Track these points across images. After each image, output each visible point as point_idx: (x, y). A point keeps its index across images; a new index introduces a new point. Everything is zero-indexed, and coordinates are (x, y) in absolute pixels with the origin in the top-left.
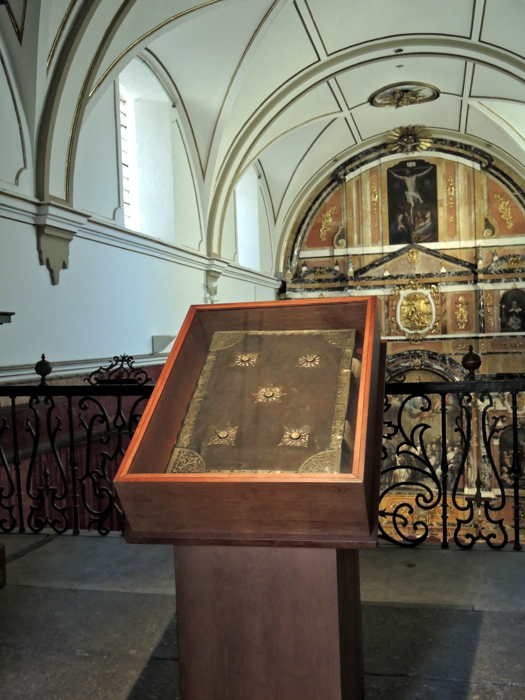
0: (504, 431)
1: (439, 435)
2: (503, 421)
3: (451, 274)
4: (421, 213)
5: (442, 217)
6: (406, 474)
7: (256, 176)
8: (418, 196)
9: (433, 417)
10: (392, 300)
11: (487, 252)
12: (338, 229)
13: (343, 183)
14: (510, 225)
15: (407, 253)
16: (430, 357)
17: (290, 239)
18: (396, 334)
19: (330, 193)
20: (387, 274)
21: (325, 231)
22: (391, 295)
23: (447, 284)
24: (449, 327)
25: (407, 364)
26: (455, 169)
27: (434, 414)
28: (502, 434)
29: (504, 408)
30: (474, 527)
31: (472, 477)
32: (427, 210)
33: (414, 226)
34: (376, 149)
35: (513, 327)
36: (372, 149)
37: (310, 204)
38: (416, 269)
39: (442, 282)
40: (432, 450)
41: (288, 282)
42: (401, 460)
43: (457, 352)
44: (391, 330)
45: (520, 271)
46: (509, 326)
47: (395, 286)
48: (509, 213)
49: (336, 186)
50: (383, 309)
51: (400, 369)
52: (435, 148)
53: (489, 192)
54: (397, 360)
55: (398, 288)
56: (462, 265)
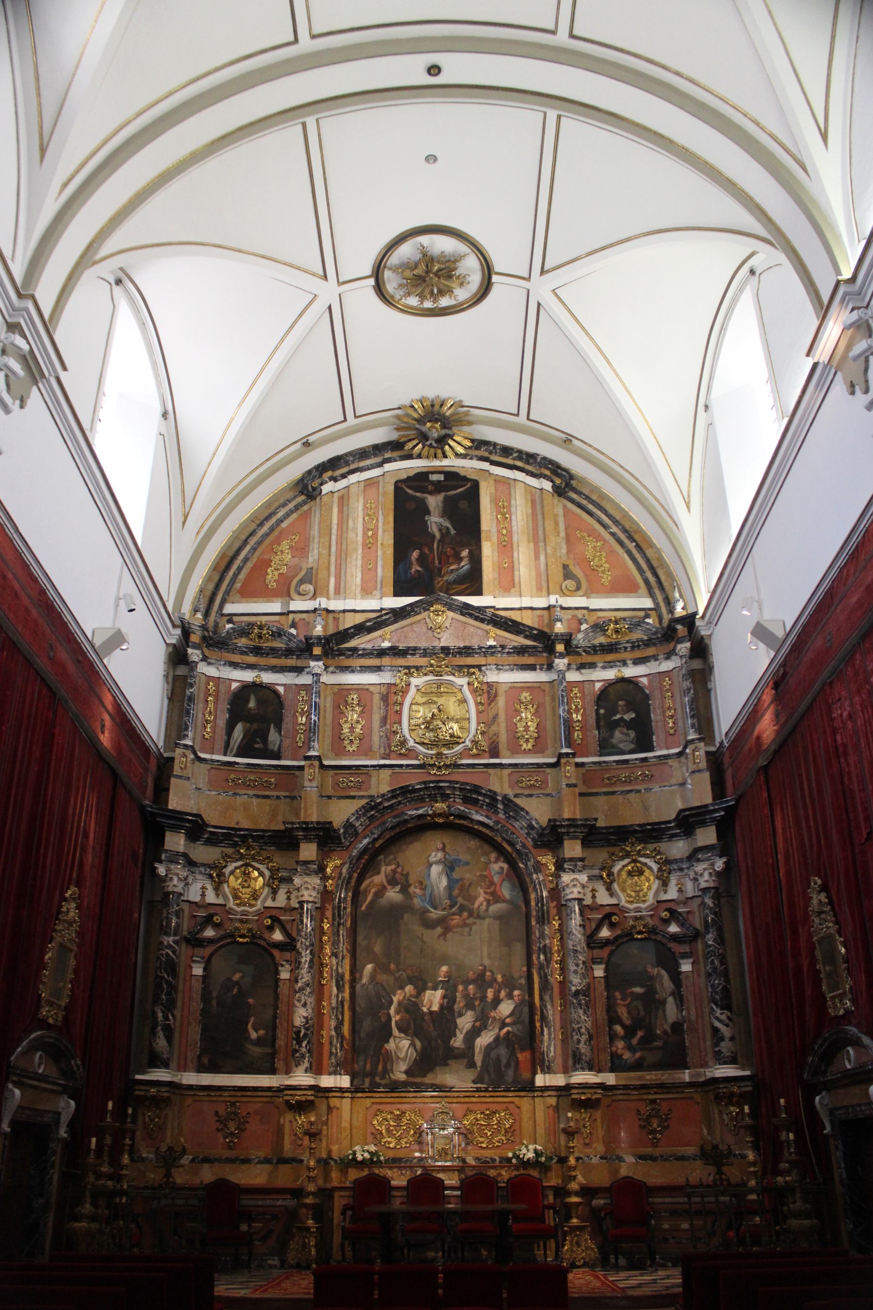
0: (614, 948)
1: (481, 965)
2: (612, 926)
4: (452, 548)
5: (488, 557)
7: (159, 411)
8: (447, 524)
9: (470, 926)
10: (395, 693)
11: (570, 617)
12: (301, 569)
14: (606, 579)
15: (426, 613)
16: (466, 800)
17: (208, 579)
18: (402, 756)
19: (291, 512)
20: (386, 644)
21: (276, 573)
23: (500, 669)
25: (421, 812)
26: (509, 488)
28: (612, 953)
29: (613, 901)
30: (558, 1162)
31: (552, 1049)
32: (464, 546)
33: (440, 570)
34: (377, 449)
35: (622, 746)
37: (253, 526)
38: (442, 640)
40: (466, 996)
41: (193, 633)
42: (401, 1020)
44: (390, 746)
46: (613, 746)
48: (604, 560)
49: (304, 503)
50: (375, 709)
51: (406, 821)
52: (477, 456)
53: (567, 528)
54: (400, 803)
56: (526, 637)
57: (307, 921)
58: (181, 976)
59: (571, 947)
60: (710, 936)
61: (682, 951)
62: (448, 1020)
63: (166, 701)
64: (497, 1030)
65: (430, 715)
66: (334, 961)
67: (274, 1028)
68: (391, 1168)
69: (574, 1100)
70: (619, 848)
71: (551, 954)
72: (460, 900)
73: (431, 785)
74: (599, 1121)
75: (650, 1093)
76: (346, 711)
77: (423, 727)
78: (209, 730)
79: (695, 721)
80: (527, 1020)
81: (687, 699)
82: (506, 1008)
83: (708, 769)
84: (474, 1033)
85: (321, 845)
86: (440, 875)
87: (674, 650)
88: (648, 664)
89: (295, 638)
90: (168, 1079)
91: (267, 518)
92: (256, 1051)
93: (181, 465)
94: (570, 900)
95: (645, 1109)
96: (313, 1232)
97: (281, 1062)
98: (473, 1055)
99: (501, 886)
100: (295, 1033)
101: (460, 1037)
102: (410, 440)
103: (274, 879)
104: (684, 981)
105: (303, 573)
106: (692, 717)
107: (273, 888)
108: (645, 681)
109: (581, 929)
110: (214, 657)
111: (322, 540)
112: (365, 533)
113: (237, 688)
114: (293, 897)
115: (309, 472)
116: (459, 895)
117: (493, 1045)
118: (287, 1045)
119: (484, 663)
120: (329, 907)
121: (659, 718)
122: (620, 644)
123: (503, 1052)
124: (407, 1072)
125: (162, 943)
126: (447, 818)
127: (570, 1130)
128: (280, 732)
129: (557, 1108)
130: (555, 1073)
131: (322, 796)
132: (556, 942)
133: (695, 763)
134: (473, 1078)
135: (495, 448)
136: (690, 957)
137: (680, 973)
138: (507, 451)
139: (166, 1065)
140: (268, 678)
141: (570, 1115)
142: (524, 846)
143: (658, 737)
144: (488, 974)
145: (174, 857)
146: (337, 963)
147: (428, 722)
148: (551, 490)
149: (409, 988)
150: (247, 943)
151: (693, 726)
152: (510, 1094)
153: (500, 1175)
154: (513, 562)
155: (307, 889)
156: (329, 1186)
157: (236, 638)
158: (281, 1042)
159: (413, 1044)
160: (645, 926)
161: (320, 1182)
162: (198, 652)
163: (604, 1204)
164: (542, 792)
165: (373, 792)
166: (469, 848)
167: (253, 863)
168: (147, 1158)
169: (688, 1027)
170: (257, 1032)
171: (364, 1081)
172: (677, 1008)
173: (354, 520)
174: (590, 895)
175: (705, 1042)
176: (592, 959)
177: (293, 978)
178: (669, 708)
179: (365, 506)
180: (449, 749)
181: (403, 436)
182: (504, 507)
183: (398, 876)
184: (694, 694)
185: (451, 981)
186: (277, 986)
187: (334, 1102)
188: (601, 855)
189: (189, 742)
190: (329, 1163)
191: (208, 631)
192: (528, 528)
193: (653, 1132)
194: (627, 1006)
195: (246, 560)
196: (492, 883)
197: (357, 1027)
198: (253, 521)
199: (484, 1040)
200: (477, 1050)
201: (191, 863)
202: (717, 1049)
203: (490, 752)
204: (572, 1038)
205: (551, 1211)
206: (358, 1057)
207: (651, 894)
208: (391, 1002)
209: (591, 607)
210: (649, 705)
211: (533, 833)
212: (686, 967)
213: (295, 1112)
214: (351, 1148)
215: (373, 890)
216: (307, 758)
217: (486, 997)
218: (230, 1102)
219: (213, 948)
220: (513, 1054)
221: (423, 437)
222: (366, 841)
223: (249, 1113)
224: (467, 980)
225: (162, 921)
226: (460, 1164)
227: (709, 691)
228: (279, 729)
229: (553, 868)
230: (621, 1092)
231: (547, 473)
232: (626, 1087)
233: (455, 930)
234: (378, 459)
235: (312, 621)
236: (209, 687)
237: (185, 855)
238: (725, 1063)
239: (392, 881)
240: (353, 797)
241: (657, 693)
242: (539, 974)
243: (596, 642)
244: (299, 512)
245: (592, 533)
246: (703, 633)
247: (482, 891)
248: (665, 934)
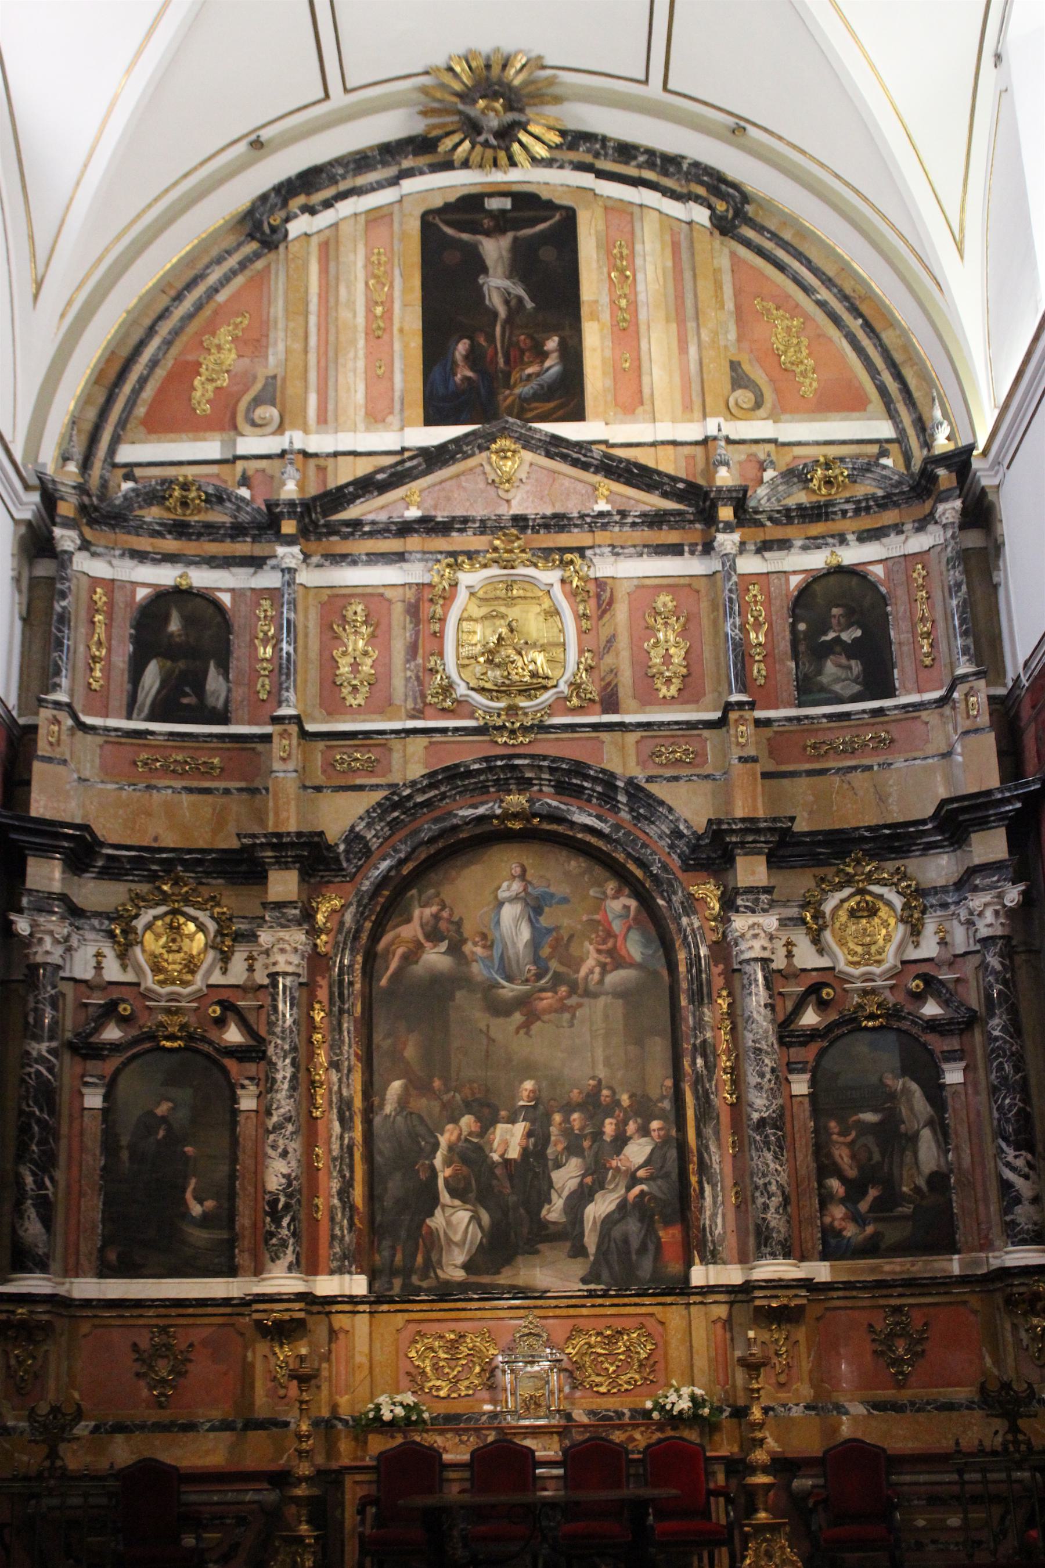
1: (593, 1078)
2: (823, 1005)
3: (630, 520)
4: (531, 337)
5: (594, 350)
8: (520, 291)
9: (572, 1010)
10: (431, 600)
11: (743, 457)
12: (255, 378)
13: (277, 247)
14: (809, 386)
15: (485, 454)
16: (562, 789)
17: (85, 400)
18: (445, 712)
19: (234, 273)
20: (413, 513)
22: (430, 585)
23: (617, 554)
24: (625, 693)
25: (481, 810)
26: (632, 222)
27: (573, 1000)
28: (822, 1053)
29: (824, 962)
30: (731, 1416)
31: (719, 1221)
33: (507, 375)
34: (389, 151)
35: (837, 688)
36: (376, 153)
37: (164, 301)
38: (514, 503)
39: (600, 546)
40: (567, 1132)
41: (62, 499)
44: (423, 696)
45: (850, 506)
46: (822, 689)
47: (439, 557)
48: (805, 352)
49: (257, 256)
50: (396, 630)
51: (455, 828)
52: (571, 162)
53: (737, 293)
55: (451, 560)
56: (665, 495)
57: (284, 1007)
58: (65, 1112)
59: (750, 1043)
60: (996, 1021)
61: (945, 1048)
62: (536, 1174)
63: (18, 625)
64: (623, 1191)
65: (495, 639)
66: (334, 1076)
67: (232, 1196)
68: (442, 1432)
69: (758, 1309)
70: (834, 869)
71: (716, 1056)
72: (554, 965)
73: (499, 763)
75: (891, 1296)
76: (343, 634)
77: (482, 660)
78: (98, 674)
79: (970, 641)
81: (954, 602)
83: (992, 726)
84: (582, 1196)
85: (305, 876)
86: (517, 922)
87: (932, 514)
88: (885, 540)
89: (248, 503)
90: (48, 1290)
91: (190, 285)
92: (200, 1236)
93: (24, 187)
94: (748, 961)
95: (883, 1323)
96: (310, 1545)
97: (246, 1255)
98: (582, 1234)
99: (625, 938)
100: (269, 1203)
102: (448, 134)
103: (223, 935)
104: (949, 1100)
105: (258, 386)
106: (965, 634)
107: (222, 952)
108: (879, 570)
109: (768, 1012)
110: (103, 542)
111: (291, 325)
112: (369, 310)
113: (144, 598)
114: (258, 966)
115: (264, 198)
116: (551, 957)
117: (616, 1216)
118: (255, 1225)
119: (589, 543)
120: (323, 982)
121: (905, 637)
122: (834, 505)
123: (633, 1227)
125: (28, 1053)
126: (528, 821)
127: (752, 1360)
128: (226, 674)
129: (728, 1323)
130: (724, 1263)
131: (305, 787)
132: (724, 1036)
133: (968, 716)
134: (581, 1273)
136: (961, 1059)
137: (943, 1086)
138: (626, 151)
139: (42, 1266)
140: (201, 578)
141: (751, 1334)
142: (665, 867)
143: (902, 672)
144: (605, 1092)
145: (44, 903)
146: (340, 1080)
147: (490, 652)
148: (707, 223)
149: (467, 1122)
150: (178, 1049)
151: (965, 651)
152: (647, 1300)
153: (631, 1439)
154: (639, 359)
155: (282, 951)
156: (334, 1465)
157: (141, 508)
158: (244, 1220)
159: (475, 1218)
160: (880, 1006)
161: (320, 1460)
162: (73, 534)
163: (813, 1486)
164: (698, 771)
165: (396, 778)
167: (186, 909)
168: (14, 1428)
169: (957, 1181)
170: (201, 1204)
171: (391, 1283)
172: (939, 1147)
173: (348, 288)
174: (783, 952)
175: (987, 1208)
176: (788, 1064)
177: (262, 1109)
178: (922, 619)
179: (368, 261)
180: (530, 698)
181: (434, 127)
182: (622, 258)
183: (443, 925)
185: (541, 1107)
186: (234, 1123)
187: (341, 1321)
188: (801, 882)
189: (62, 697)
190: (333, 1427)
191: (89, 495)
192: (665, 295)
193: (897, 1362)
194: (851, 1145)
195: (154, 363)
196: (609, 934)
197: (378, 1191)
198: (164, 292)
200: (588, 1225)
201: (75, 912)
202: (1008, 1218)
203: (602, 702)
204: (754, 1202)
205: (722, 1500)
206: (380, 1244)
207: (891, 949)
208: (436, 1146)
209: (781, 439)
210: (887, 615)
212: (953, 1075)
213: (272, 1340)
214: (372, 1397)
215: (400, 951)
216: (276, 720)
217: (603, 1133)
218: (157, 1326)
219: (122, 1059)
220: (650, 1231)
221: (472, 128)
222: (384, 865)
223: (191, 1345)
224: (568, 1104)
225: (26, 1016)
226: (563, 1422)
227: (996, 587)
228: (224, 668)
229: (717, 907)
230: (840, 1294)
231: (701, 191)
232: (848, 1286)
233: (546, 1017)
234: (391, 171)
235: (277, 475)
236: (96, 597)
237: (64, 898)
238: (1023, 1242)
239: (434, 935)
240: (360, 788)
241: (901, 592)
242: (695, 1092)
243: (791, 502)
244: (248, 273)
245: (783, 302)
246: (984, 482)
247: (591, 948)
248: (916, 1019)
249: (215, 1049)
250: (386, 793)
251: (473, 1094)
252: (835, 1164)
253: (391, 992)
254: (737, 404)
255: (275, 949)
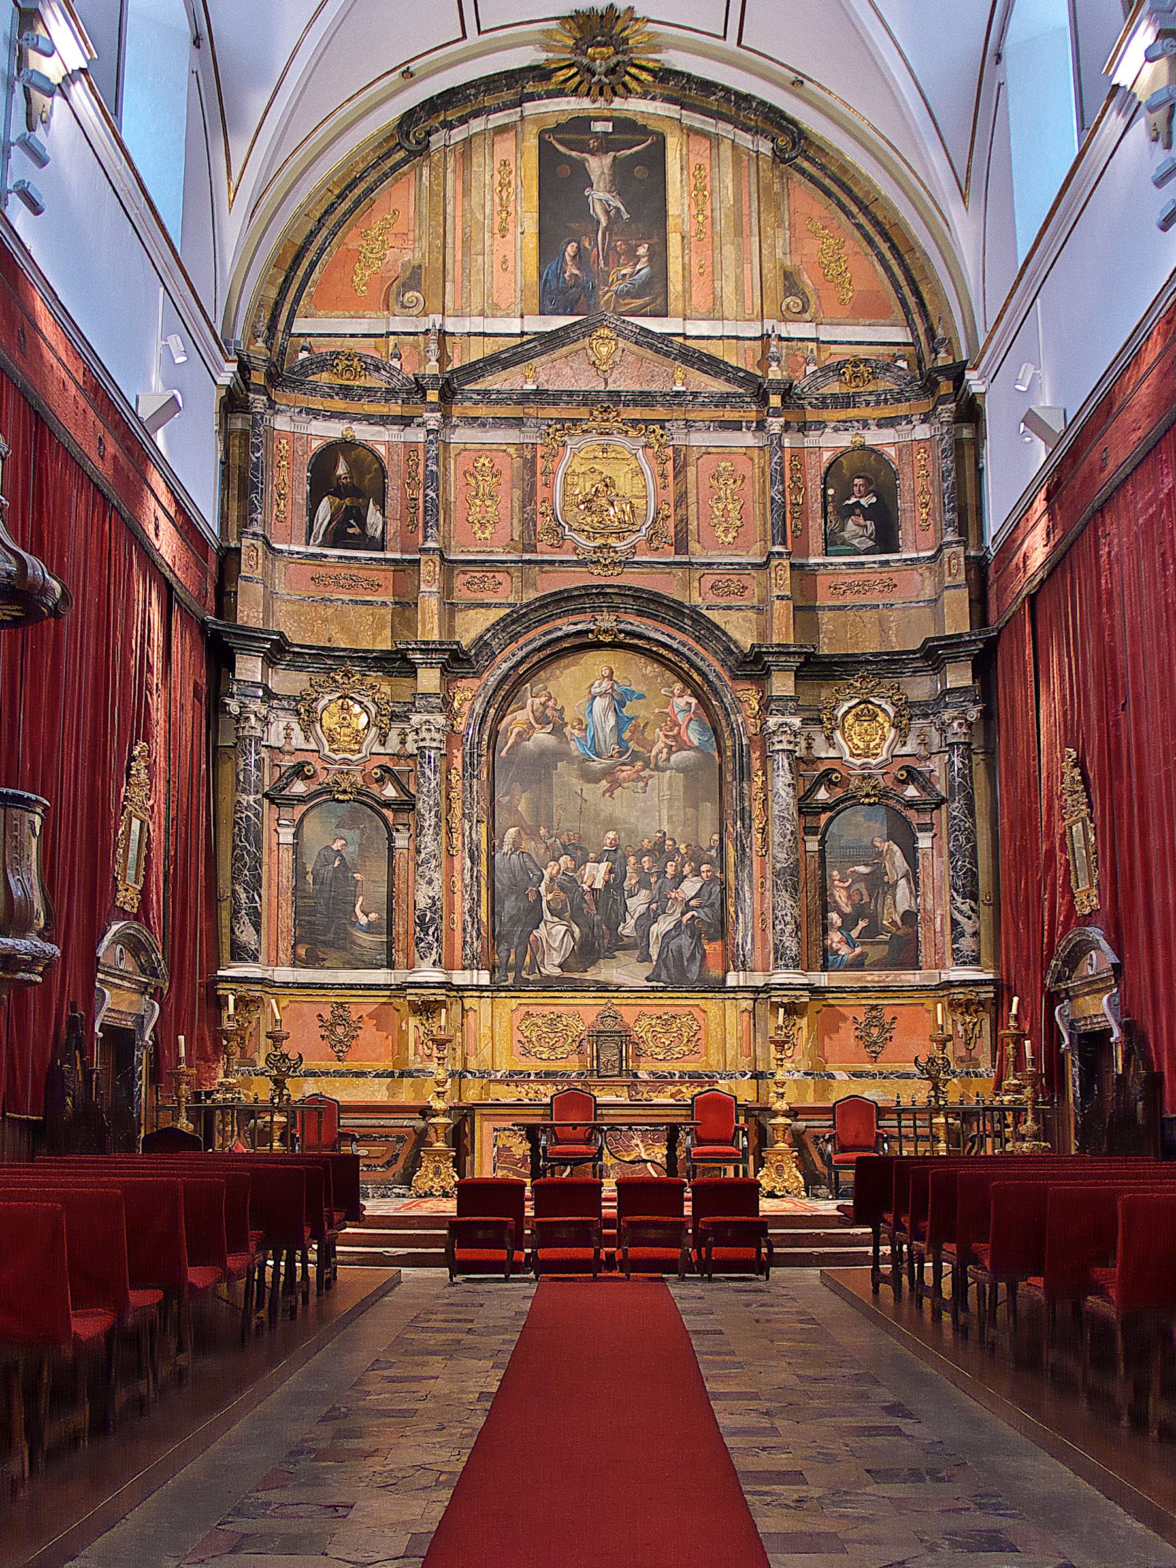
1: (659, 831)
2: (831, 784)
4: (625, 242)
6: (568, 938)
15: (587, 340)
20: (530, 386)
25: (580, 627)
28: (831, 819)
29: (832, 753)
30: (751, 1078)
31: (749, 940)
35: (855, 542)
40: (639, 871)
43: (712, 599)
45: (872, 398)
49: (405, 161)
55: (558, 426)
56: (728, 380)
58: (265, 845)
67: (390, 911)
74: (805, 1030)
77: (582, 507)
80: (717, 905)
82: (690, 887)
92: (364, 938)
101: (631, 922)
107: (381, 728)
108: (892, 452)
109: (790, 790)
123: (685, 941)
124: (560, 966)
132: (757, 805)
135: (688, 82)
138: (707, 86)
140: (362, 432)
144: (669, 842)
147: (590, 501)
149: (565, 860)
155: (429, 730)
158: (399, 929)
159: (569, 931)
166: (644, 676)
172: (911, 893)
174: (803, 744)
177: (412, 848)
183: (549, 712)
184: (957, 477)
185: (620, 852)
187: (468, 1003)
190: (465, 1077)
199: (660, 927)
211: (731, 661)
212: (924, 841)
215: (516, 731)
219: (305, 808)
229: (757, 708)
236: (281, 446)
239: (542, 720)
241: (907, 469)
243: (826, 391)
248: (899, 798)
249: (376, 801)
250: (508, 611)
251: (570, 840)
252: (835, 901)
253: (508, 762)
254: (788, 307)
255: (424, 727)
